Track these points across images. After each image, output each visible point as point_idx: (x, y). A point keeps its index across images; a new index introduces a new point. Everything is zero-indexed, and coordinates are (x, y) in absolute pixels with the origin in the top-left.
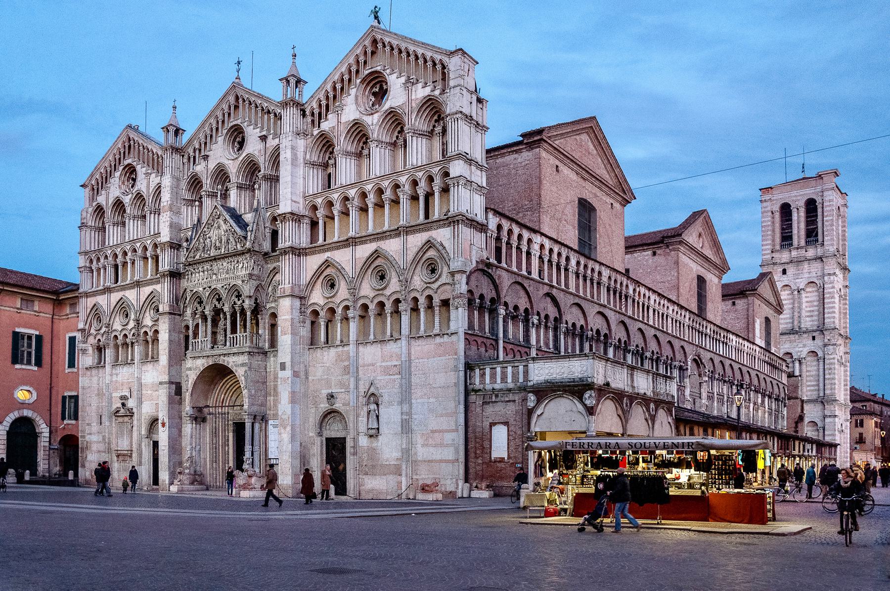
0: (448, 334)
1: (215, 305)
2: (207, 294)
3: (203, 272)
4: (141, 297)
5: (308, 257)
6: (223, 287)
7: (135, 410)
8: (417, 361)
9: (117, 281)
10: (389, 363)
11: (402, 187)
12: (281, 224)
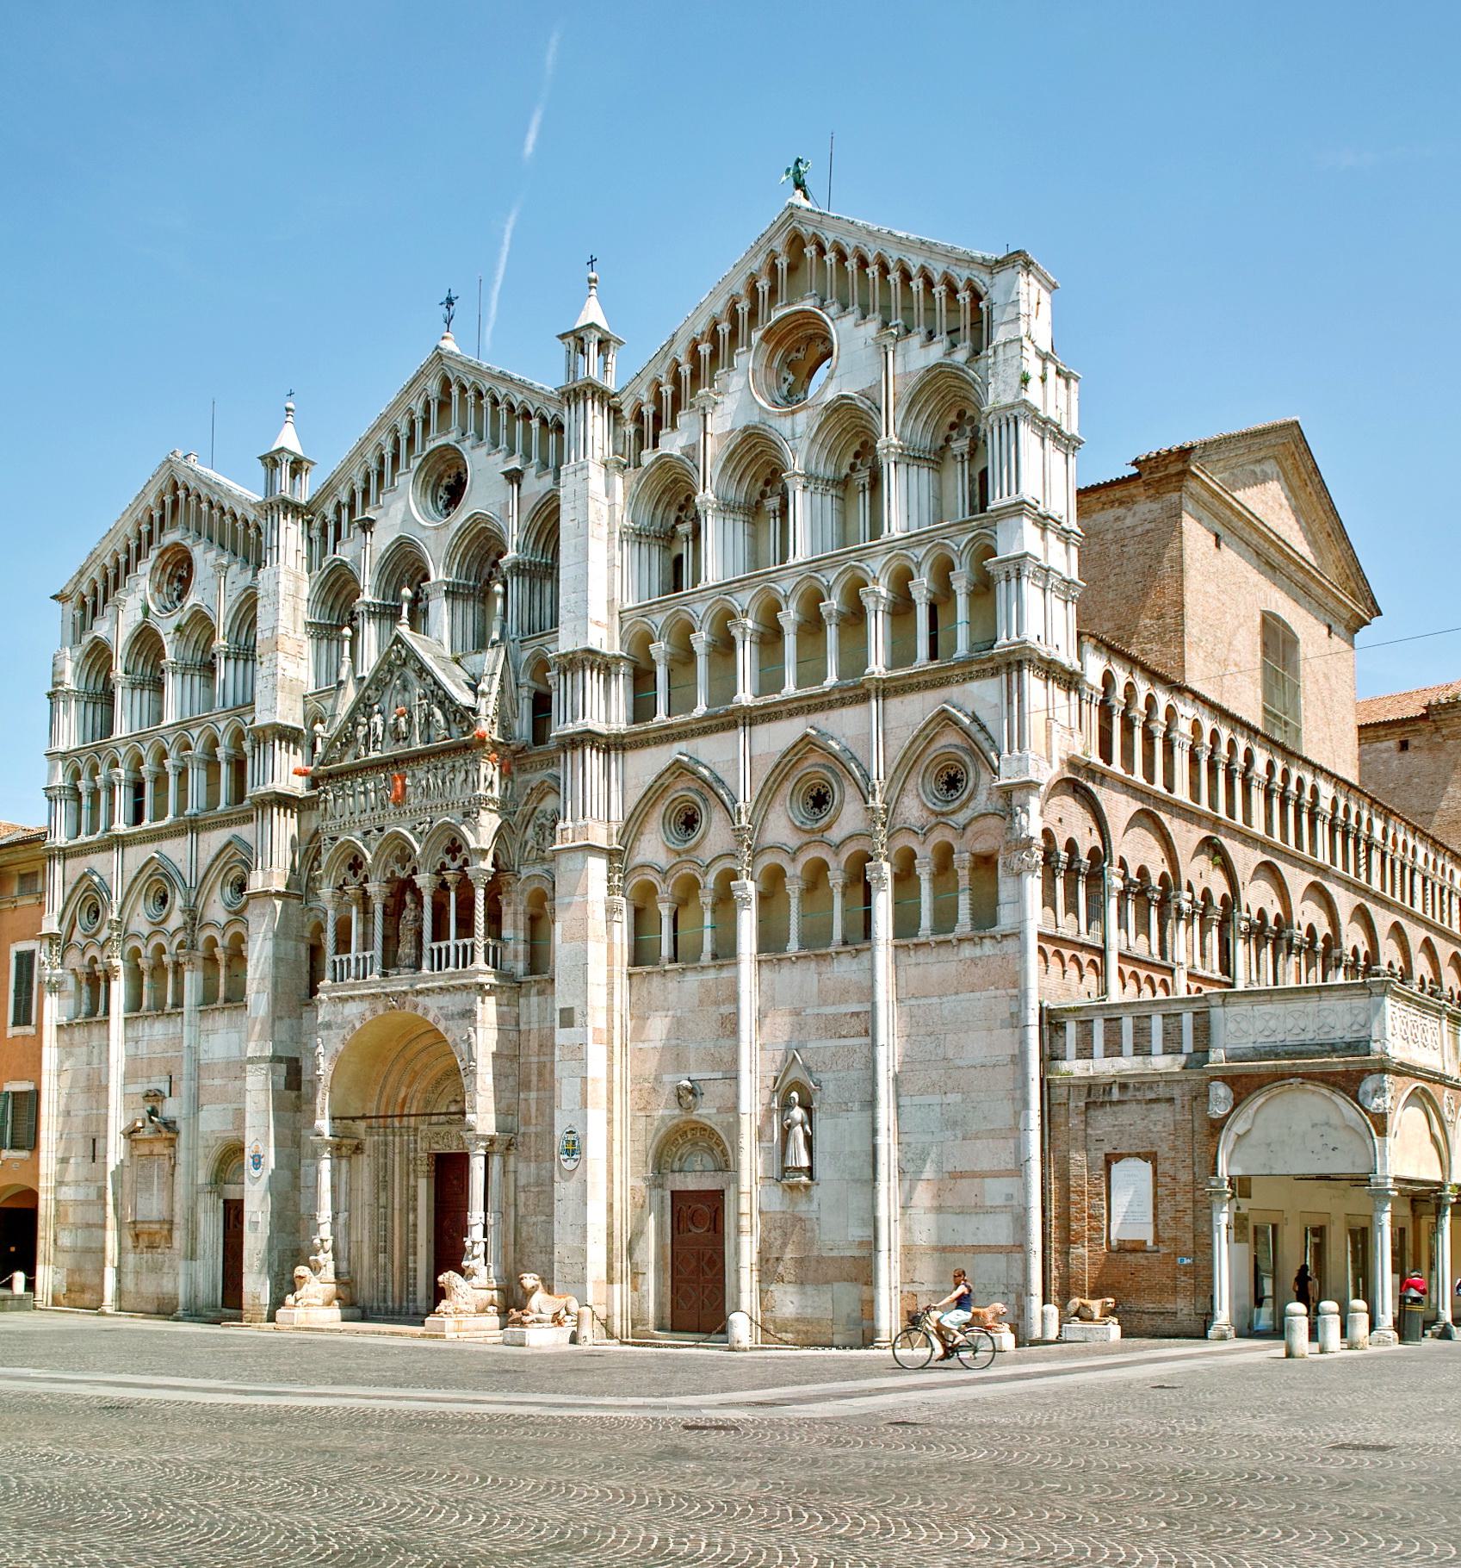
0: (993, 937)
1: (393, 872)
2: (375, 846)
3: (365, 793)
4: (201, 855)
5: (629, 754)
7: (182, 1126)
8: (913, 1002)
9: (138, 818)
11: (870, 583)
12: (562, 677)
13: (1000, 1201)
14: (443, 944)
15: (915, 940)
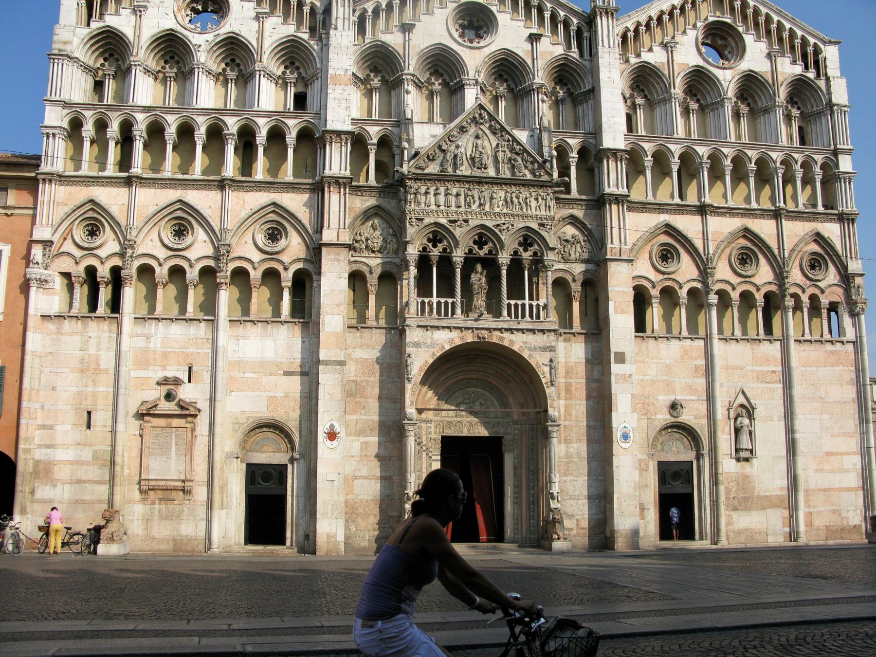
6: (498, 225)
8: (803, 368)
10: (766, 368)
13: (851, 466)
14: (520, 302)
15: (804, 339)
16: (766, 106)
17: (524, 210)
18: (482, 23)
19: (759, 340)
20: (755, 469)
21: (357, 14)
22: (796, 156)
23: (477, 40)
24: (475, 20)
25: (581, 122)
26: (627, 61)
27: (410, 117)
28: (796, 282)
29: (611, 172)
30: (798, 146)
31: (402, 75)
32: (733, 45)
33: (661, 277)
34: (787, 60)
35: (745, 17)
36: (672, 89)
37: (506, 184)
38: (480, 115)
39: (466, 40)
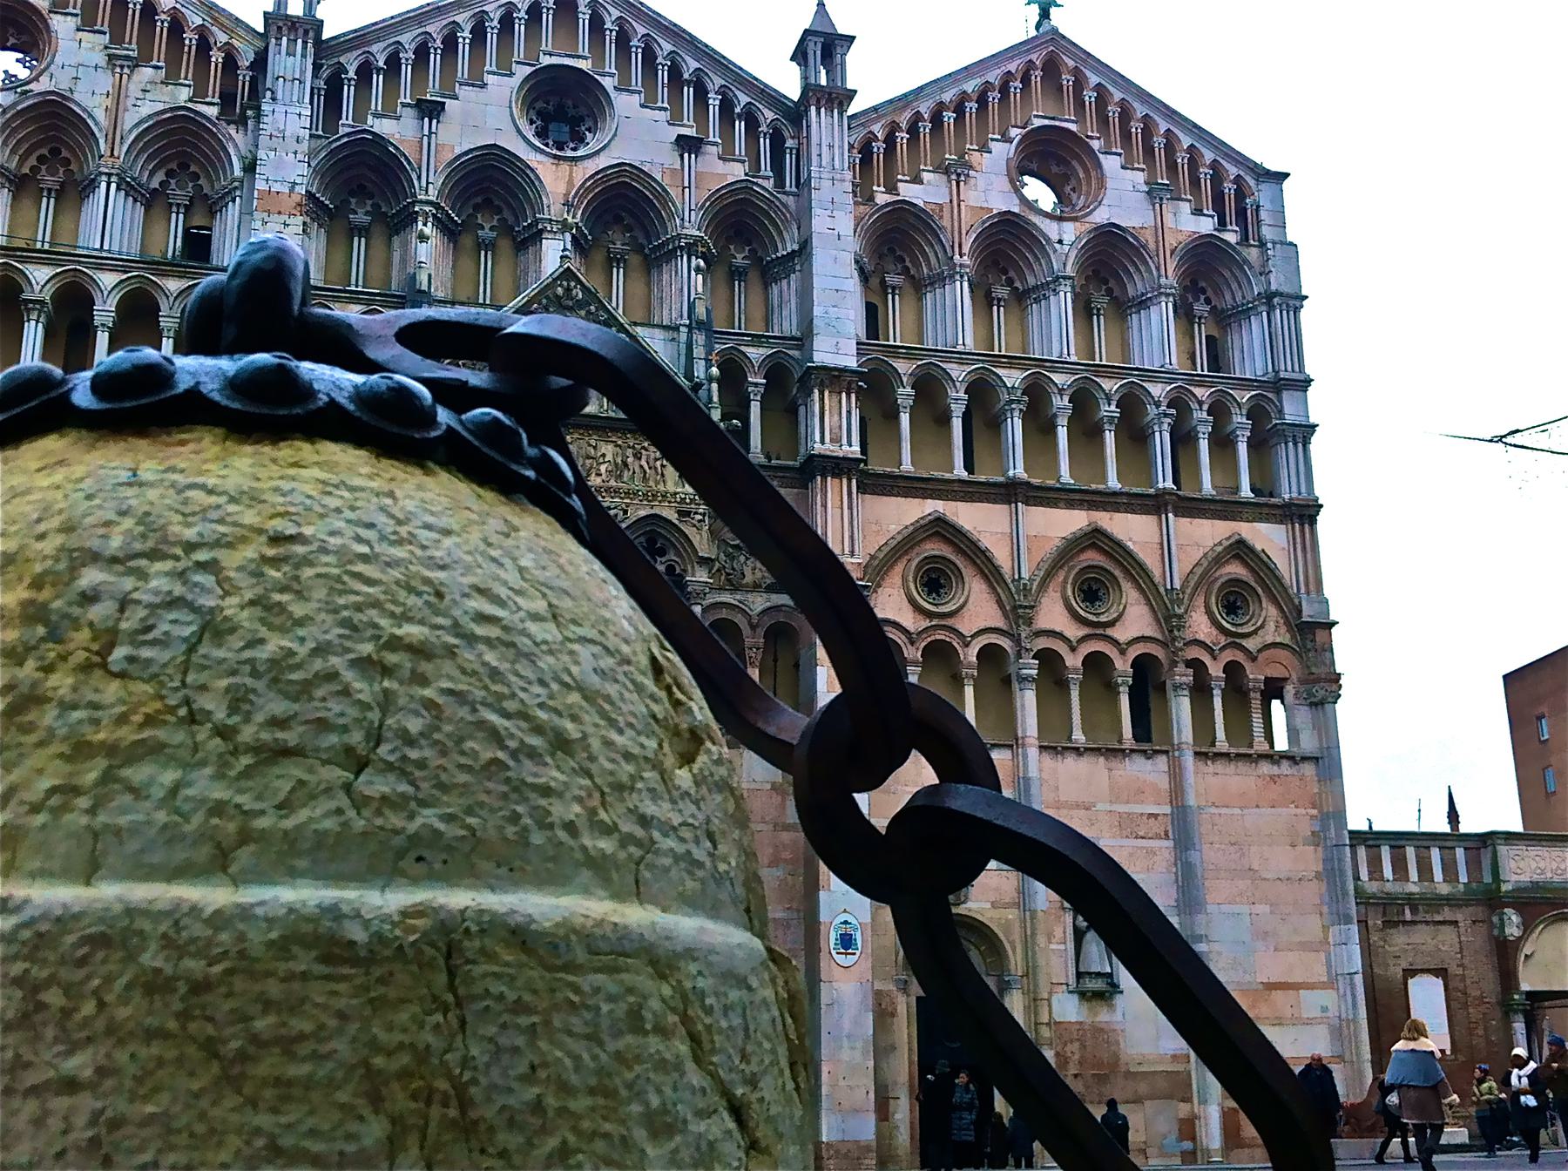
8: (1213, 810)
10: (1138, 809)
13: (1318, 1014)
16: (1143, 294)
17: (651, 483)
18: (583, 111)
19: (1124, 750)
20: (1118, 1017)
21: (325, 72)
22: (1198, 392)
23: (572, 145)
24: (570, 103)
25: (775, 316)
26: (871, 199)
27: (424, 287)
28: (1197, 637)
29: (827, 413)
30: (1206, 373)
31: (413, 204)
32: (1082, 175)
33: (927, 623)
34: (1185, 208)
35: (1103, 121)
36: (957, 257)
37: (614, 430)
38: (568, 290)
39: (551, 143)
